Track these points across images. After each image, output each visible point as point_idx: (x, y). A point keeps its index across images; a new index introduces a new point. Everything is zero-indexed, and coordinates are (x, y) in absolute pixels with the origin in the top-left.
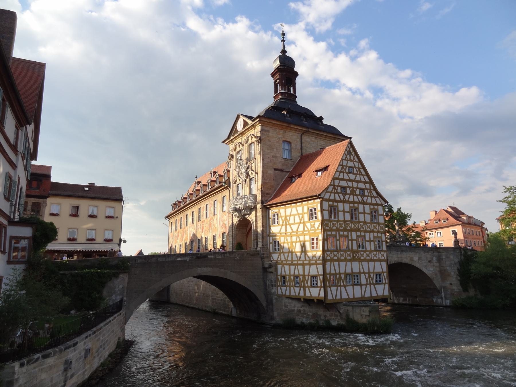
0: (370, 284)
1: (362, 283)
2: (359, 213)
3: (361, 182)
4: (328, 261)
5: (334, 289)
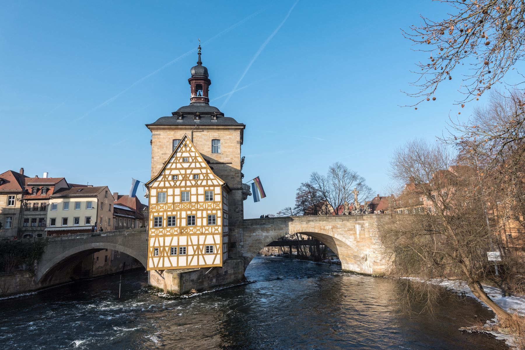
0: (198, 255)
1: (189, 254)
2: (191, 195)
3: (196, 168)
4: (153, 236)
5: (156, 260)
